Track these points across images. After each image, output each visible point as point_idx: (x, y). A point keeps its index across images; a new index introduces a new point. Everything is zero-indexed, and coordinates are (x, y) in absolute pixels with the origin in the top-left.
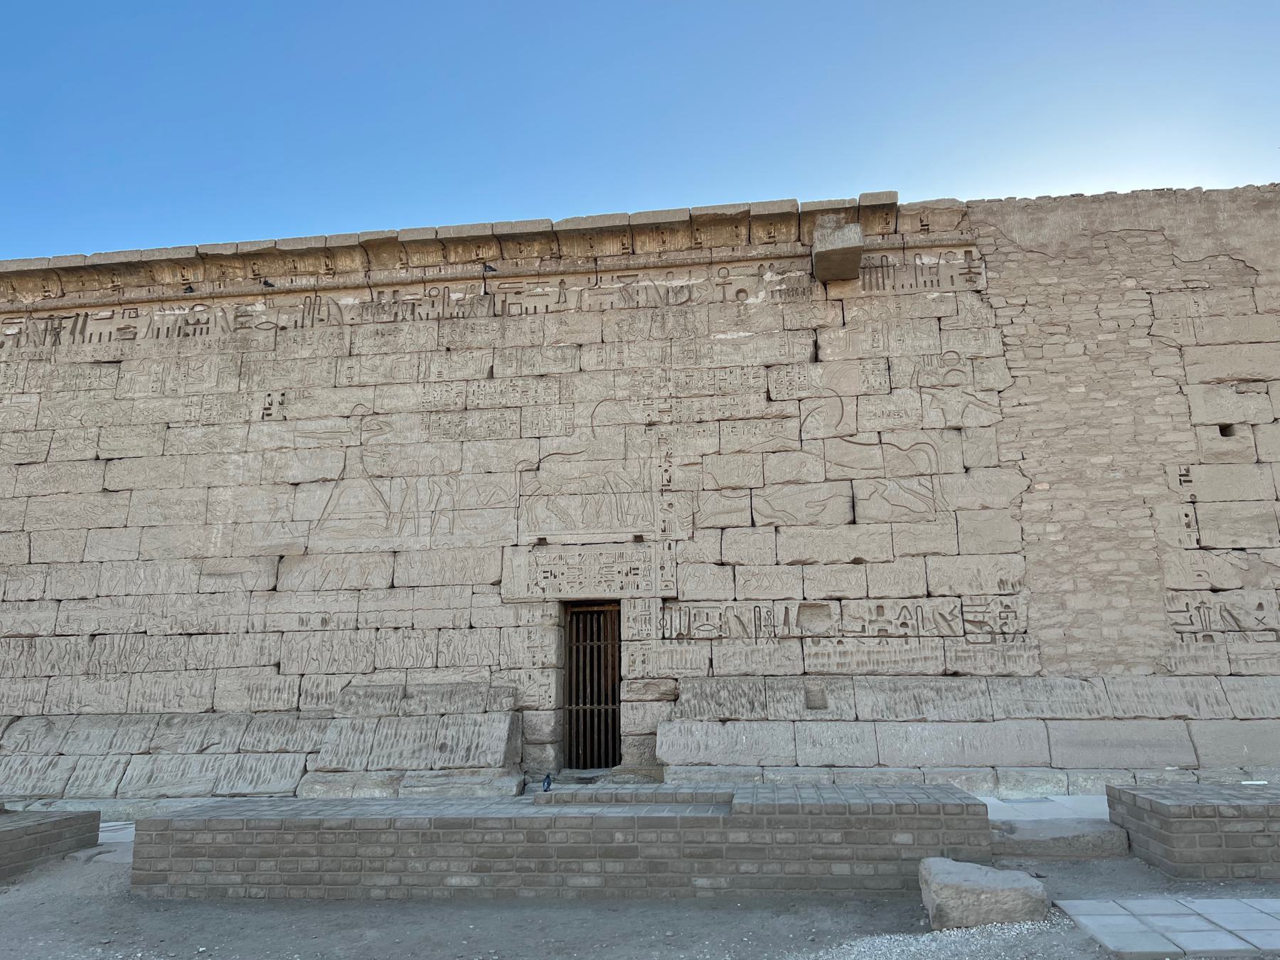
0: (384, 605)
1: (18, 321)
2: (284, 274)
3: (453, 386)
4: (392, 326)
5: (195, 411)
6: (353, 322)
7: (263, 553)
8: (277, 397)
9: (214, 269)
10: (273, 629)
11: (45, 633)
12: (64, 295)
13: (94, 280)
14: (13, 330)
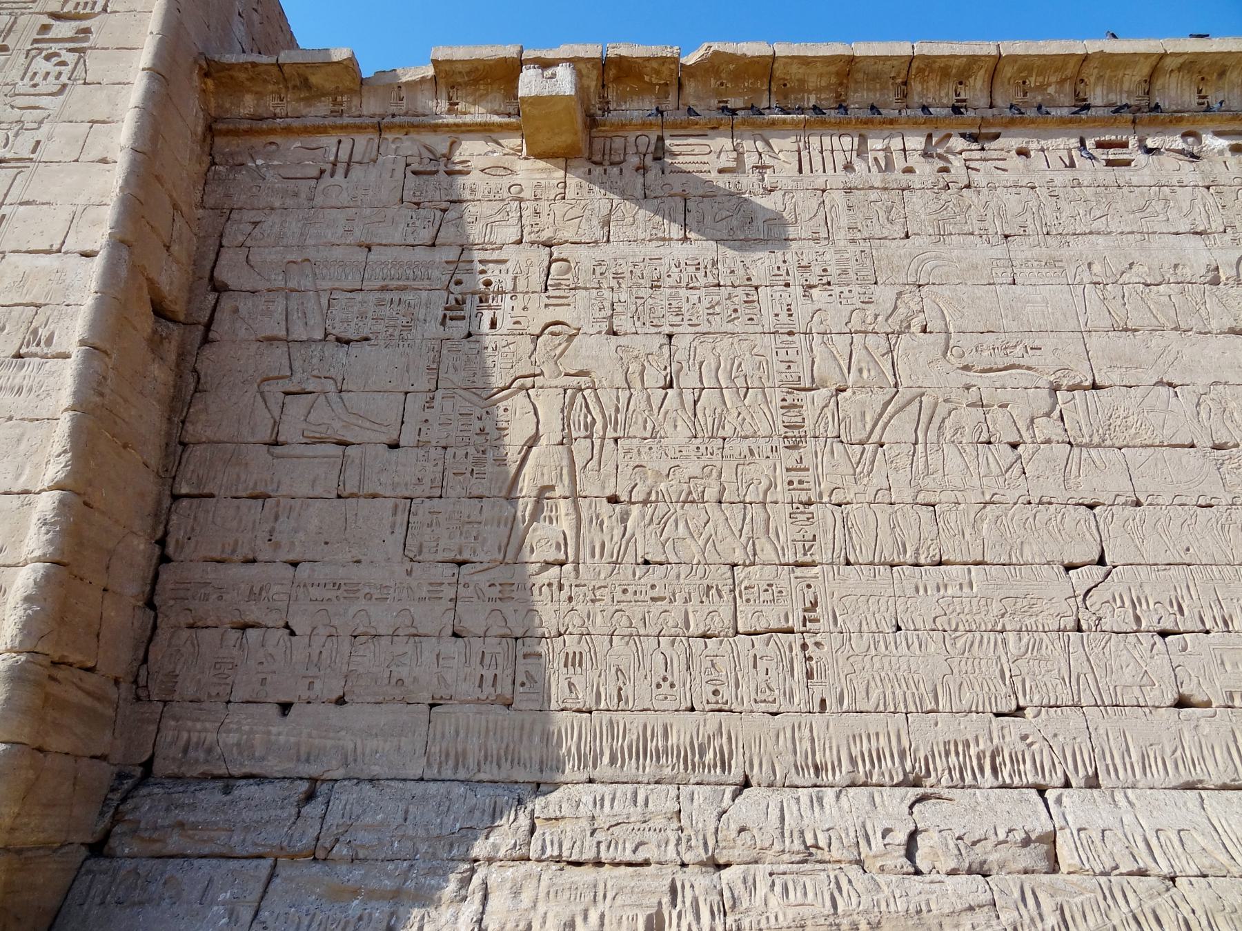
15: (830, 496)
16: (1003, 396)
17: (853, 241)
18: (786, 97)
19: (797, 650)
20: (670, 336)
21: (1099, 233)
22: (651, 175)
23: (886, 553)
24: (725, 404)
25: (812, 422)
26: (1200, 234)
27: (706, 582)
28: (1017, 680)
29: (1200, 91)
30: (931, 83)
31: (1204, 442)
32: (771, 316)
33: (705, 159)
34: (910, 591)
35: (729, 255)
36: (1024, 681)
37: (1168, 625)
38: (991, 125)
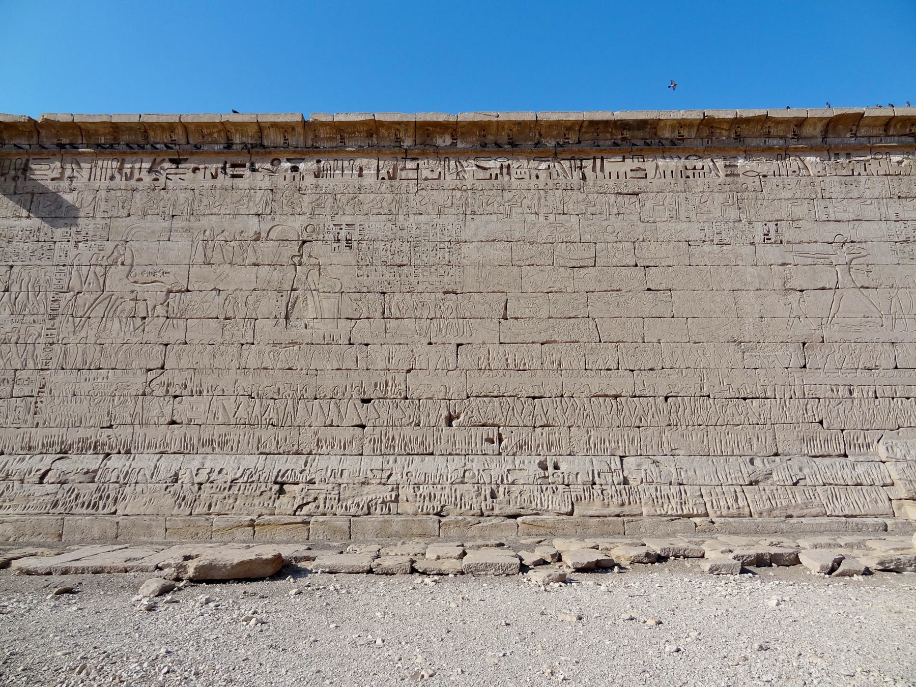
1: (547, 159)
2: (760, 136)
5: (709, 233)
6: (819, 174)
7: (789, 340)
8: (772, 226)
10: (811, 396)
11: (627, 394)
12: (579, 142)
13: (608, 132)
14: (544, 166)
15: (62, 341)
16: (146, 295)
17: (103, 218)
18: (90, 138)
19: (33, 403)
20: (12, 267)
21: (215, 214)
22: (19, 182)
23: (78, 365)
24: (28, 299)
25: (63, 307)
26: (259, 215)
27: (3, 377)
28: (113, 415)
29: (285, 137)
30: (158, 132)
31: (222, 316)
32: (58, 256)
33: (45, 172)
34: (83, 380)
35: (46, 227)
36: (116, 415)
37: (178, 393)
38: (183, 155)
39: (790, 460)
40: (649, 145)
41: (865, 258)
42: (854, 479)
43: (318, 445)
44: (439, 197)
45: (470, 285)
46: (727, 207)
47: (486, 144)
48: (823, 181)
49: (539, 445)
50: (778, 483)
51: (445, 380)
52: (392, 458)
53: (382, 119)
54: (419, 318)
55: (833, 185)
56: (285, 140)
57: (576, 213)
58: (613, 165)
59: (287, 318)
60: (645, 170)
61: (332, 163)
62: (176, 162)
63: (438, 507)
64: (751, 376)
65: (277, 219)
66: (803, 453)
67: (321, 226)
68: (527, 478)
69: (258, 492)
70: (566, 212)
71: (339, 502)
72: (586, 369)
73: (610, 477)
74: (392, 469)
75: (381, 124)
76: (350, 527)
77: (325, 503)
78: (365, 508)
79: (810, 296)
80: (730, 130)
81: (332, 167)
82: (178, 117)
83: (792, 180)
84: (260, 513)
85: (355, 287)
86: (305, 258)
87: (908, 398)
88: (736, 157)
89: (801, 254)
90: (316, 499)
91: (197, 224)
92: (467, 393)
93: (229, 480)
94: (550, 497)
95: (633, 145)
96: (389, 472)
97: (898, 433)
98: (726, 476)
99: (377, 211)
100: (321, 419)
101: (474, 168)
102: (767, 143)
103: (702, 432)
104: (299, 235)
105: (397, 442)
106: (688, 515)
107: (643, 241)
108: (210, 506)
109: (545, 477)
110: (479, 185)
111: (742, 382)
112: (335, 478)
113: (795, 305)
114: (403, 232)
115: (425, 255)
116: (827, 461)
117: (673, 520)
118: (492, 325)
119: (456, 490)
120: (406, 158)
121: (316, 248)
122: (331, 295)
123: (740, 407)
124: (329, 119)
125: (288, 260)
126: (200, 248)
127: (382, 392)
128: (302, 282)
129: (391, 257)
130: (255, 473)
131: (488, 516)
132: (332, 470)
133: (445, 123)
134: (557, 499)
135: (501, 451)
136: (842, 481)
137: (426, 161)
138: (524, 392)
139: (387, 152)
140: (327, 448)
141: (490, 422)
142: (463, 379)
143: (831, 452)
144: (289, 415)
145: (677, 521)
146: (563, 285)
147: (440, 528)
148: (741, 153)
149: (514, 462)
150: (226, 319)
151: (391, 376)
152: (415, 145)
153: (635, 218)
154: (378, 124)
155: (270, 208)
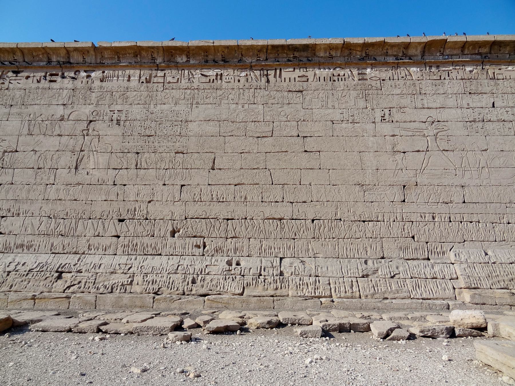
0: (462, 211)
1: (246, 70)
2: (381, 55)
3: (476, 110)
4: (440, 81)
5: (346, 116)
6: (419, 79)
7: (395, 184)
8: (387, 112)
9: (346, 51)
12: (267, 59)
13: (284, 53)
14: (243, 74)
26: (64, 105)
29: (83, 57)
30: (6, 54)
31: (36, 167)
37: (4, 215)
38: (21, 69)
39: (391, 261)
40: (309, 60)
41: (446, 132)
42: (432, 275)
43: (89, 248)
44: (176, 93)
45: (192, 148)
46: (359, 100)
47: (207, 61)
48: (421, 83)
49: (229, 250)
50: (381, 276)
51: (172, 208)
52: (133, 257)
53: (141, 45)
54: (159, 169)
55: (427, 86)
56: (84, 59)
57: (262, 103)
58: (288, 73)
59: (76, 168)
60: (307, 77)
61: (111, 72)
62: (16, 73)
63: (156, 289)
64: (368, 207)
65: (75, 107)
66: (400, 257)
67: (102, 111)
68: (217, 271)
69: (44, 278)
70: (255, 102)
71: (94, 285)
72: (262, 202)
73: (272, 271)
74: (132, 264)
75: (141, 48)
76: (96, 301)
77: (85, 285)
78: (110, 288)
79: (410, 156)
80: (362, 51)
81: (112, 75)
82: (16, 45)
83: (401, 82)
84: (42, 291)
85: (120, 149)
86: (90, 131)
87: (471, 222)
88: (366, 69)
89: (405, 129)
90: (80, 282)
91: (26, 110)
92: (186, 216)
93: (28, 270)
94: (230, 283)
95: (300, 61)
96: (130, 266)
97: (464, 245)
98: (348, 271)
99: (137, 102)
100: (92, 231)
101: (200, 76)
102: (386, 60)
103: (334, 243)
104: (88, 117)
105: (139, 247)
106: (318, 296)
107: (304, 121)
108: (11, 286)
109: (229, 270)
110: (202, 86)
111: (362, 210)
112: (95, 269)
113: (400, 161)
114: (153, 115)
115: (166, 130)
116: (415, 262)
117: (306, 299)
118: (204, 173)
119: (170, 278)
120: (158, 70)
121: (97, 125)
122: (105, 154)
123: (361, 227)
124: (109, 45)
125: (79, 132)
126: (26, 125)
127: (132, 215)
128: (87, 146)
129: (144, 131)
130: (45, 266)
131: (188, 295)
132: (95, 264)
133: (181, 47)
134: (234, 284)
135: (204, 253)
136: (424, 276)
137: (170, 72)
138: (221, 216)
139: (146, 66)
140: (94, 250)
141: (198, 234)
142: (183, 207)
143: (419, 257)
144: (72, 229)
145: (310, 300)
146: (251, 149)
147: (154, 302)
148: (369, 66)
149: (211, 261)
150: (39, 169)
151: (138, 205)
152: (164, 62)
153: (299, 106)
154: (139, 48)
155: (71, 101)
